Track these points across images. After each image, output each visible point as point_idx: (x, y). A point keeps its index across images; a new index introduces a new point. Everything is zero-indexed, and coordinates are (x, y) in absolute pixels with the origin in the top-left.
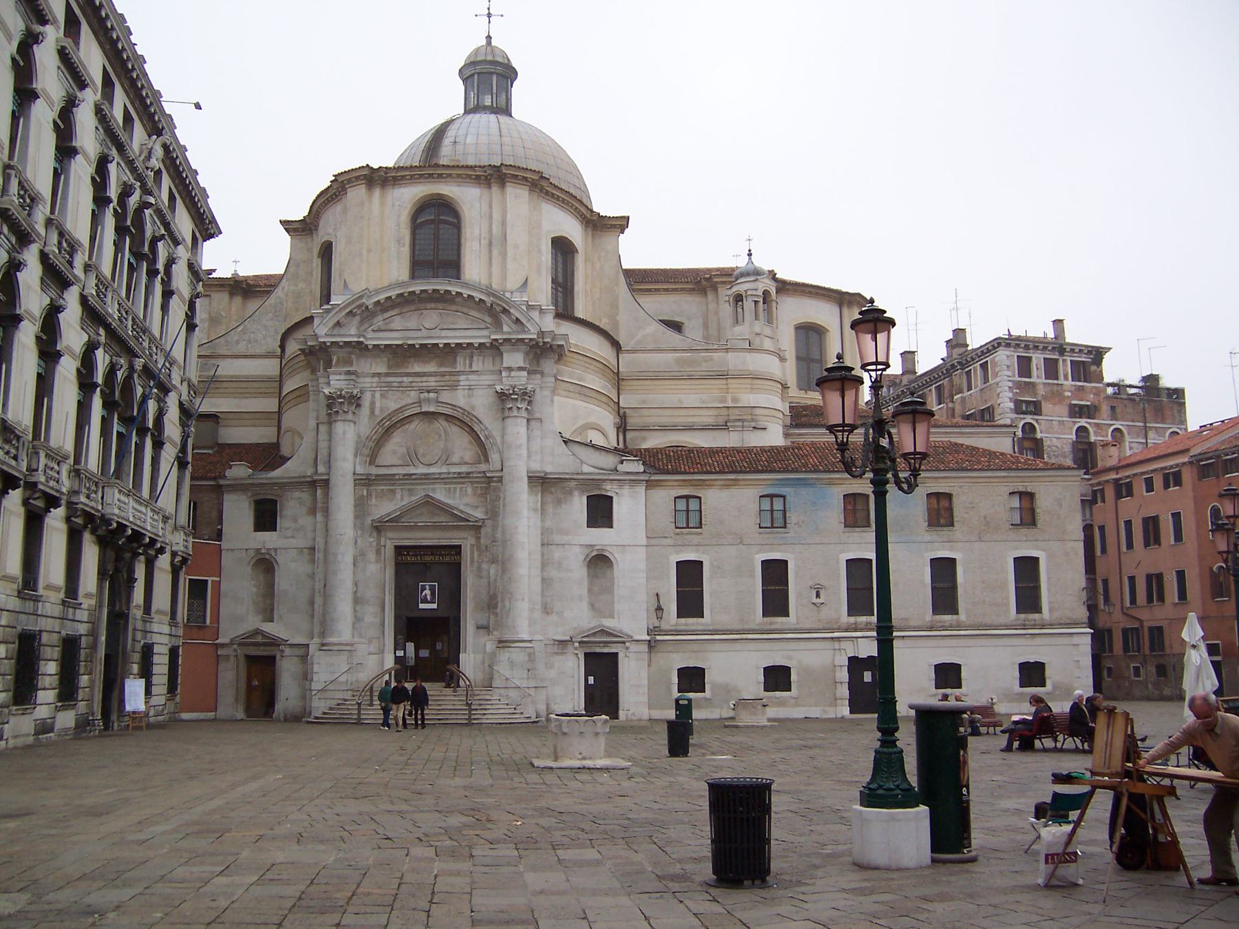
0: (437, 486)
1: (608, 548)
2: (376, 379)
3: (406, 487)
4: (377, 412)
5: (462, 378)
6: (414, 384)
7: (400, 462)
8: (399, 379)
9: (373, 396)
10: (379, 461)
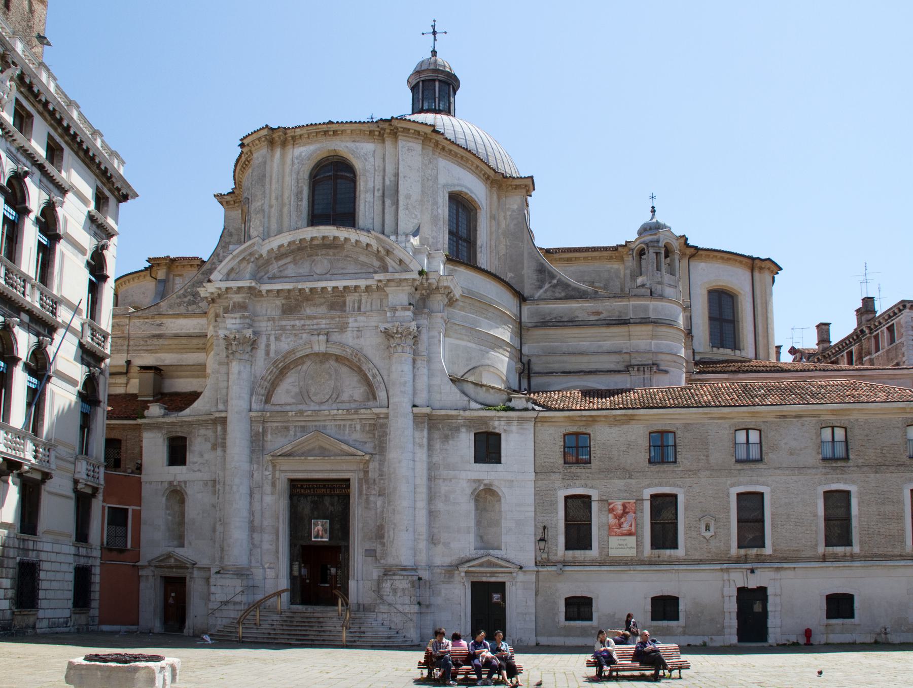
3: (300, 424)
7: (294, 401)
10: (274, 399)
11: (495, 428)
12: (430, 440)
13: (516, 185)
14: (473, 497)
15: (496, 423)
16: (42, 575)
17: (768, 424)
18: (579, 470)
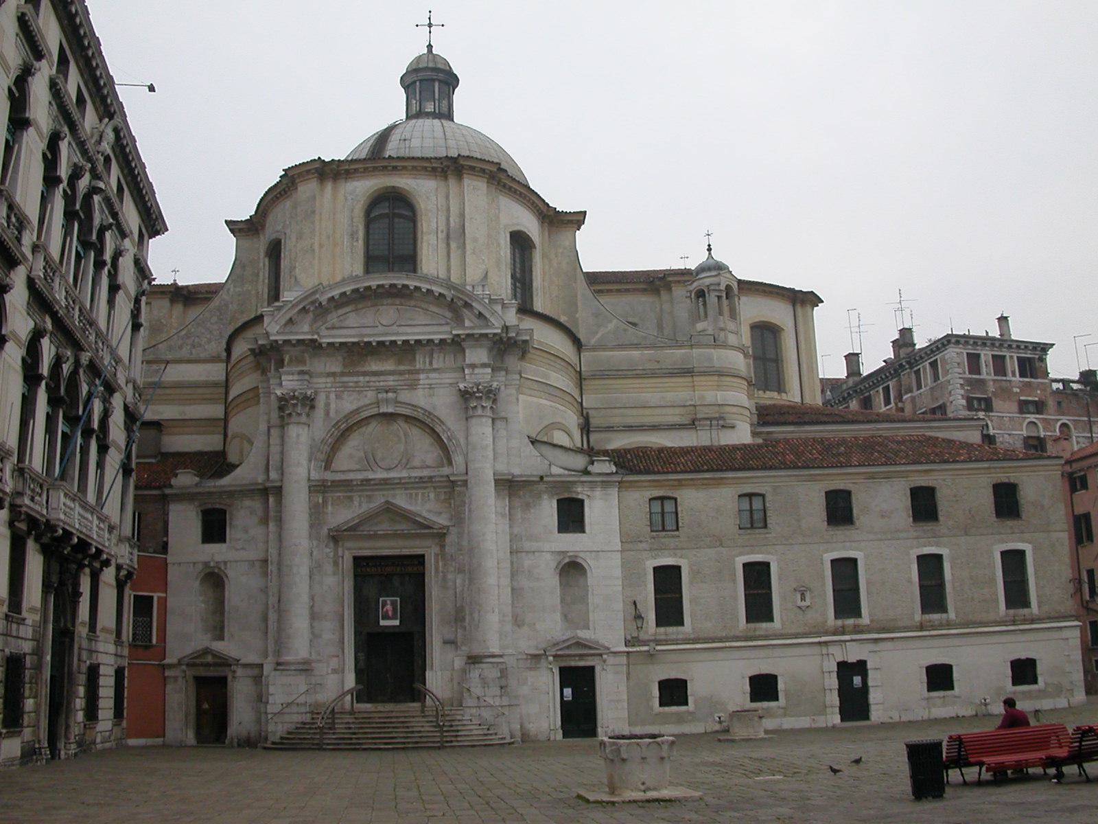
0: (398, 492)
1: (581, 555)
2: (330, 380)
4: (332, 413)
5: (422, 376)
6: (372, 384)
7: (357, 467)
8: (355, 379)
9: (328, 397)
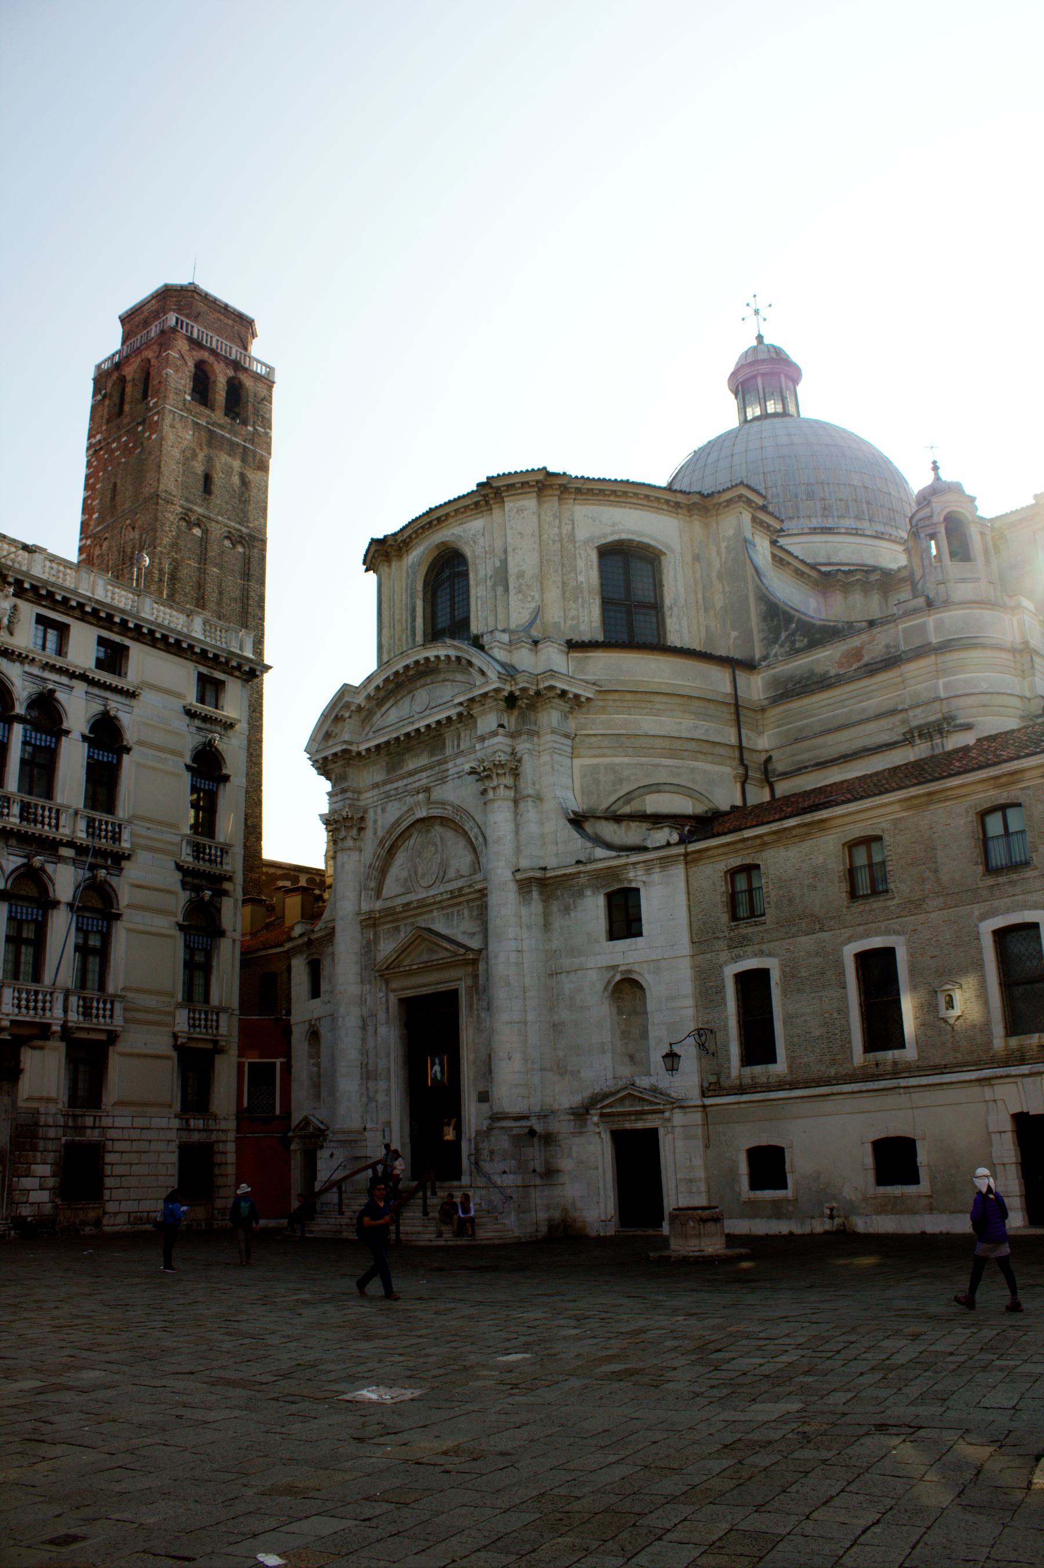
1: (636, 968)
2: (376, 792)
5: (450, 765)
6: (410, 787)
7: (403, 890)
8: (395, 785)
9: (375, 812)
10: (386, 893)
11: (631, 881)
12: (546, 915)
13: (727, 501)
14: (606, 994)
15: (631, 875)
16: (109, 1158)
17: (1031, 793)
18: (750, 930)
